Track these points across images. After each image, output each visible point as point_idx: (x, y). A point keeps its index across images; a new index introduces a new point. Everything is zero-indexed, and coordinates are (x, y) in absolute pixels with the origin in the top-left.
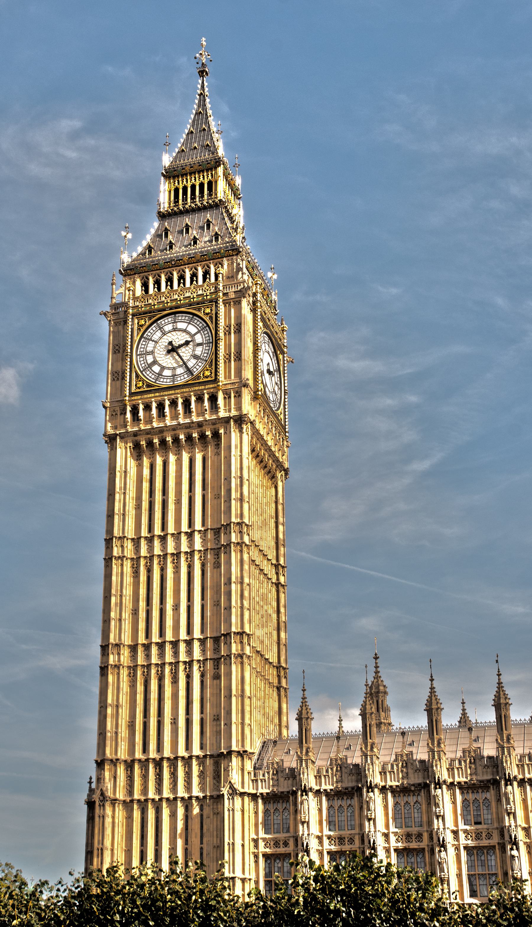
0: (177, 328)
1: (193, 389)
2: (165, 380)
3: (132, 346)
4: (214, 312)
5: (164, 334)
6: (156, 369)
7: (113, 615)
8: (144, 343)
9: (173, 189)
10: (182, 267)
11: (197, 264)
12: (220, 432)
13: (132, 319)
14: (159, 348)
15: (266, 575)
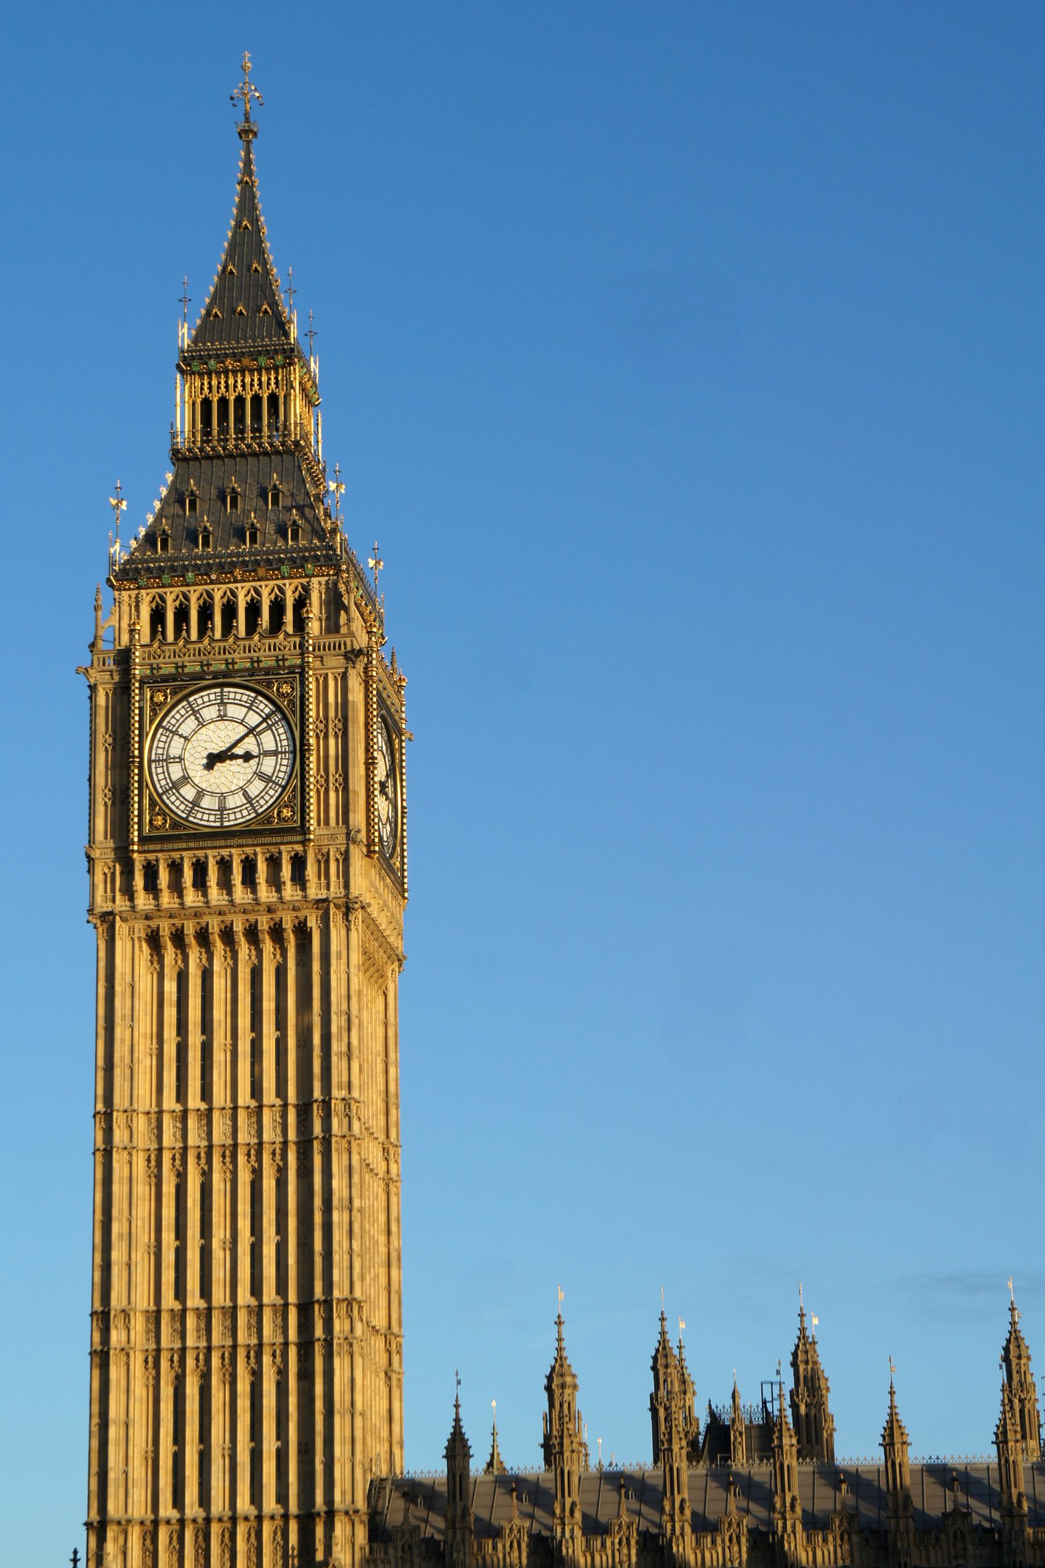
0: (225, 715)
1: (259, 841)
2: (206, 817)
3: (141, 743)
4: (297, 693)
5: (202, 724)
6: (188, 792)
7: (114, 1255)
8: (163, 738)
9: (199, 401)
10: (231, 586)
11: (259, 583)
12: (309, 925)
13: (141, 688)
14: (193, 751)
15: (372, 1170)
